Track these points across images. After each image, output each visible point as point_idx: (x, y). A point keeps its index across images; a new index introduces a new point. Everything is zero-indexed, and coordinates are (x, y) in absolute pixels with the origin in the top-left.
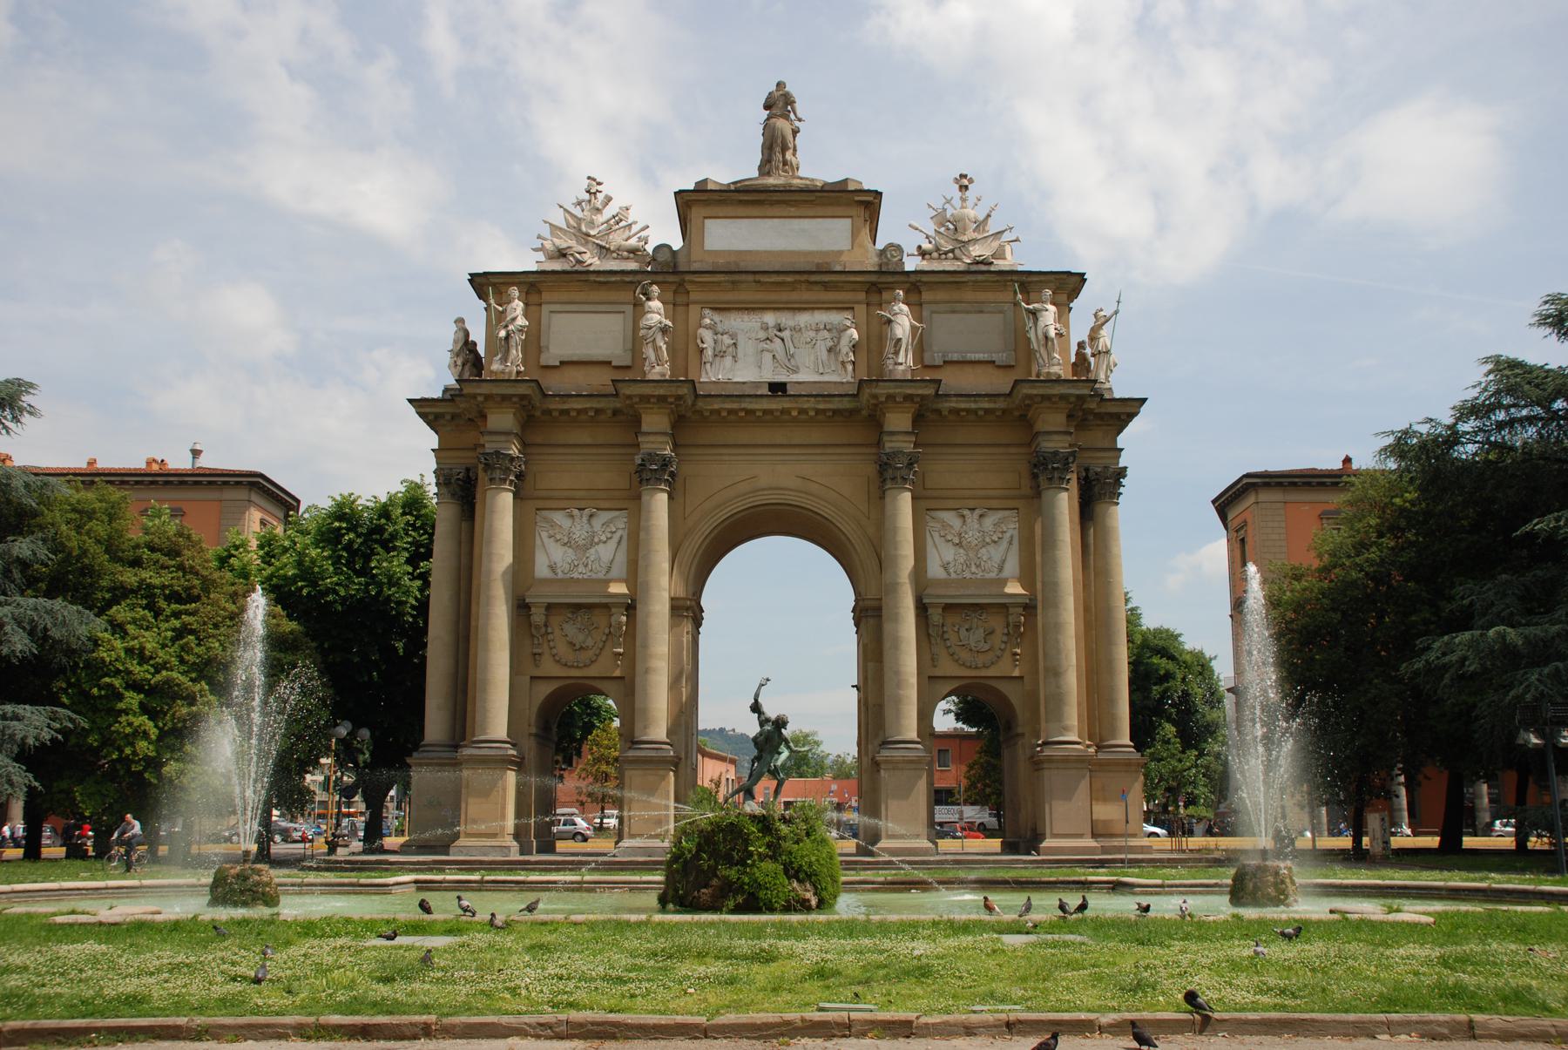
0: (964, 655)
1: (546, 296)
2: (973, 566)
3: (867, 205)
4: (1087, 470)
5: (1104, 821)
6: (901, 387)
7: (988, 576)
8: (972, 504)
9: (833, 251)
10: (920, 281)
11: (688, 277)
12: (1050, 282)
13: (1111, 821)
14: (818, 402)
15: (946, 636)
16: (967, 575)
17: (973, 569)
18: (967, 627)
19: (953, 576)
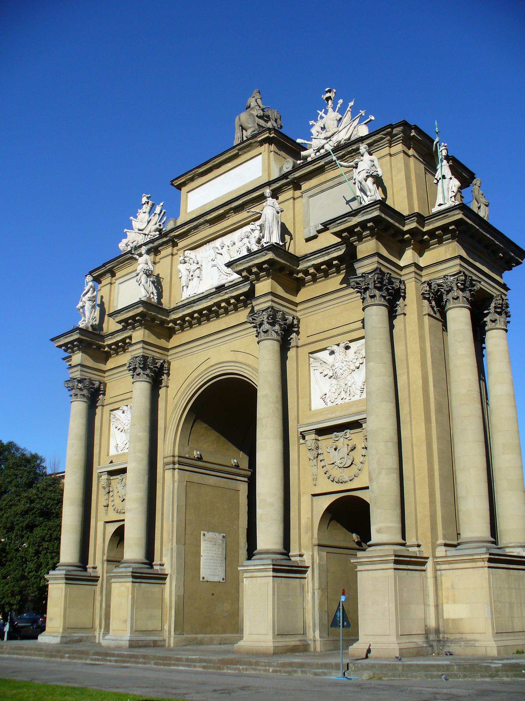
0: (336, 473)
1: (118, 275)
2: (343, 392)
3: (268, 141)
4: (429, 285)
5: (454, 620)
6: (251, 260)
7: (353, 399)
8: (337, 340)
9: (250, 182)
10: (295, 178)
11: (172, 234)
12: (382, 139)
13: (461, 619)
14: (232, 291)
15: (320, 457)
16: (339, 402)
17: (343, 395)
18: (334, 447)
19: (330, 404)
